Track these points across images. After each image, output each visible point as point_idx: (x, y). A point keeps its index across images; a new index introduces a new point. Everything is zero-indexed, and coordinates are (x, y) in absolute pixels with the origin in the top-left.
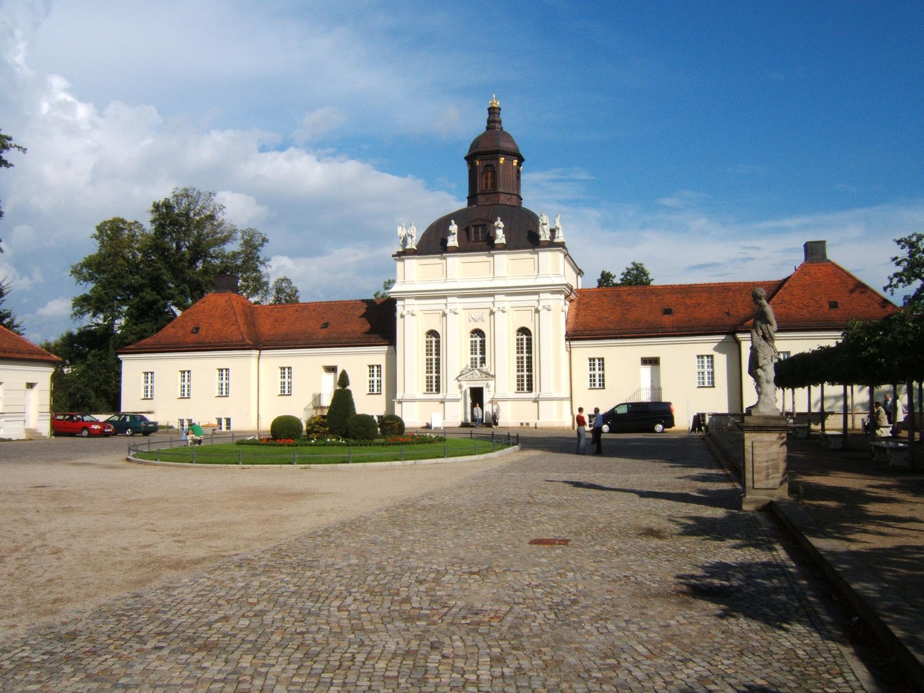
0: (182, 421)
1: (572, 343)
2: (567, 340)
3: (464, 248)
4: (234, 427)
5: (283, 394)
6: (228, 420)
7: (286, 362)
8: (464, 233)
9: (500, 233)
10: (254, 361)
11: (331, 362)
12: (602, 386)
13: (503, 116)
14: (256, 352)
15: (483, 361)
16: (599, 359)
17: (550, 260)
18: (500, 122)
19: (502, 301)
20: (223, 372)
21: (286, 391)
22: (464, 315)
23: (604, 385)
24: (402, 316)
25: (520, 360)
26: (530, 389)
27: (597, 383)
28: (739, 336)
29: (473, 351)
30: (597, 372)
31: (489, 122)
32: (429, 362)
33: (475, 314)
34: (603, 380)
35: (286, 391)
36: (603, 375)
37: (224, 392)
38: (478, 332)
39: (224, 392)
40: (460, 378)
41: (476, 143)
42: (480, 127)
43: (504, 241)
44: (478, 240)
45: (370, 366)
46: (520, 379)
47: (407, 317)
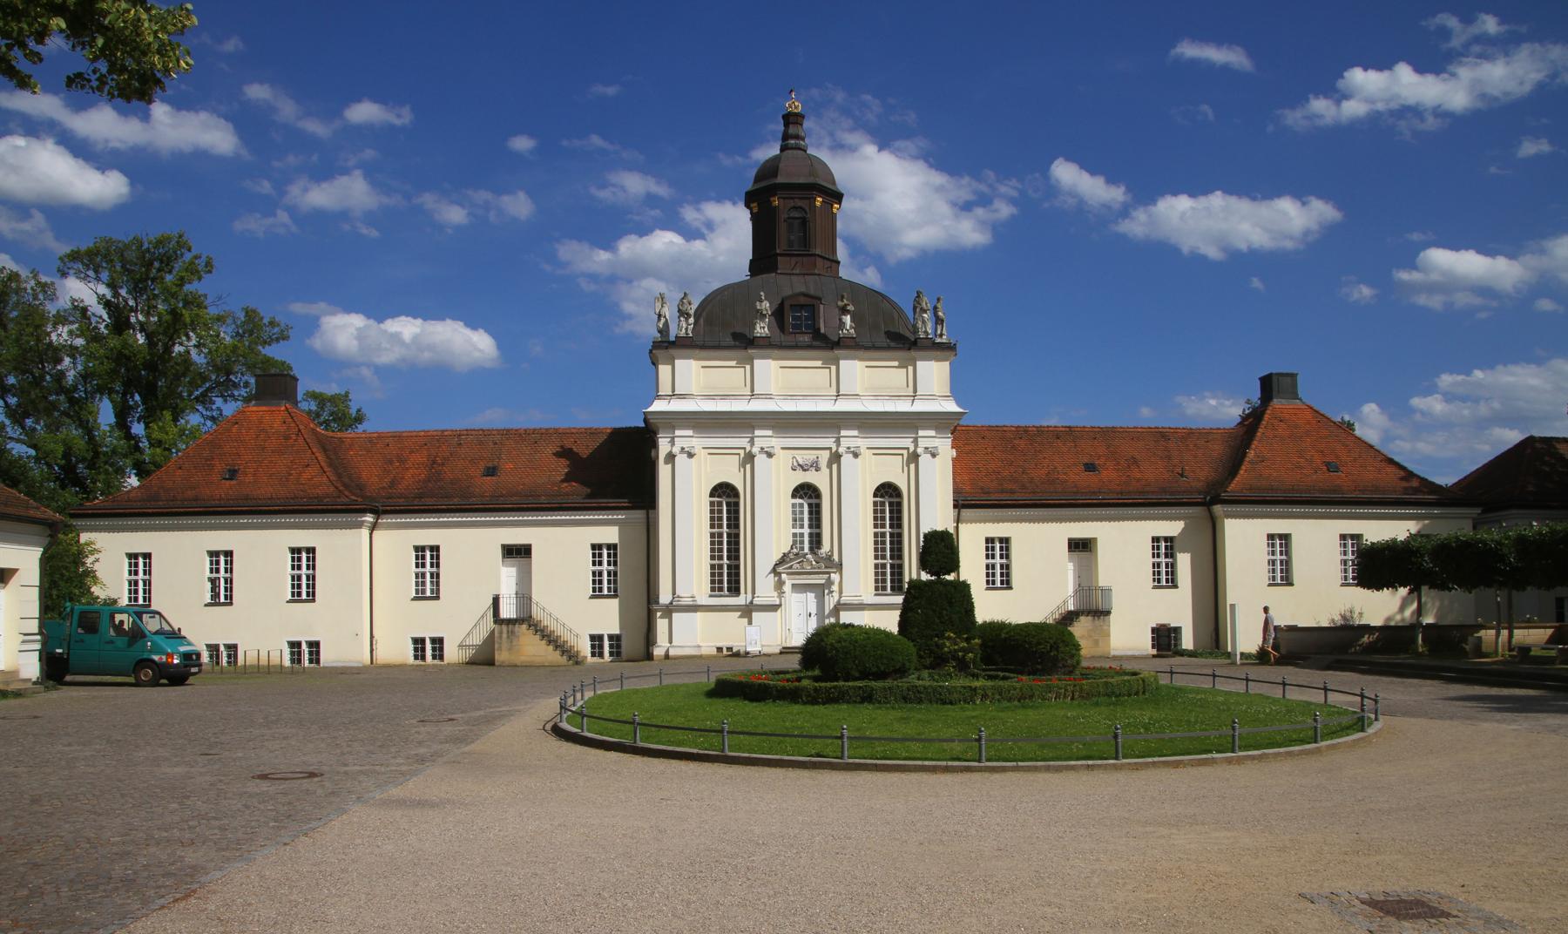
0: (295, 645)
1: (966, 513)
2: (955, 506)
4: (327, 657)
5: (420, 597)
6: (315, 646)
7: (427, 537)
8: (779, 315)
9: (847, 319)
10: (365, 532)
11: (517, 536)
12: (1007, 584)
14: (369, 518)
16: (1001, 540)
17: (934, 374)
19: (851, 438)
20: (303, 556)
21: (428, 586)
22: (783, 459)
23: (1008, 582)
24: (671, 458)
25: (879, 539)
26: (735, 589)
27: (998, 579)
28: (1218, 509)
30: (998, 561)
33: (805, 457)
34: (1008, 575)
35: (428, 586)
36: (1008, 567)
37: (304, 590)
38: (807, 492)
39: (304, 590)
40: (780, 569)
44: (805, 329)
45: (594, 547)
46: (715, 571)
47: (681, 459)
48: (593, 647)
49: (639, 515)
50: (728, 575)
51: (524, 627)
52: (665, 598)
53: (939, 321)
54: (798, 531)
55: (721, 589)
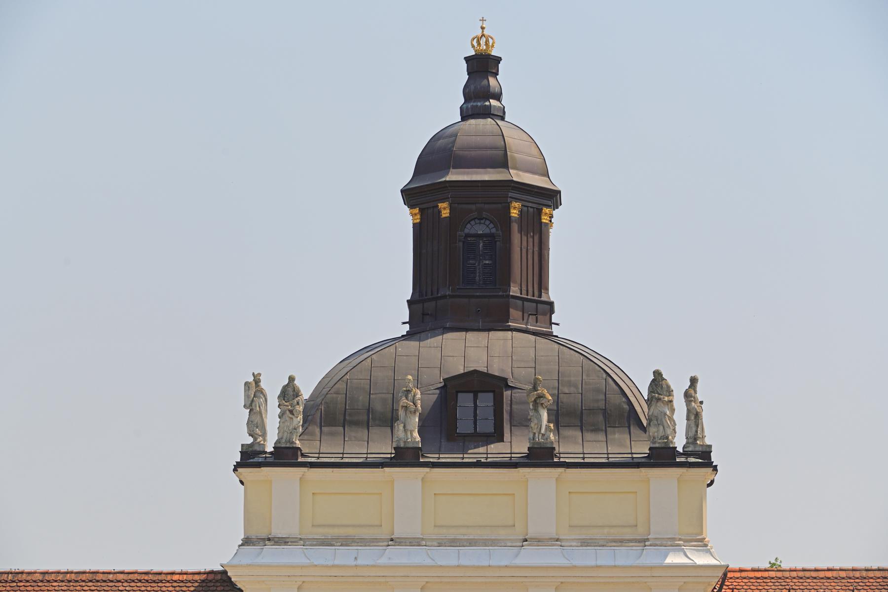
13: (505, 79)
18: (498, 97)
31: (469, 94)
41: (437, 156)
42: (445, 109)
53: (694, 417)
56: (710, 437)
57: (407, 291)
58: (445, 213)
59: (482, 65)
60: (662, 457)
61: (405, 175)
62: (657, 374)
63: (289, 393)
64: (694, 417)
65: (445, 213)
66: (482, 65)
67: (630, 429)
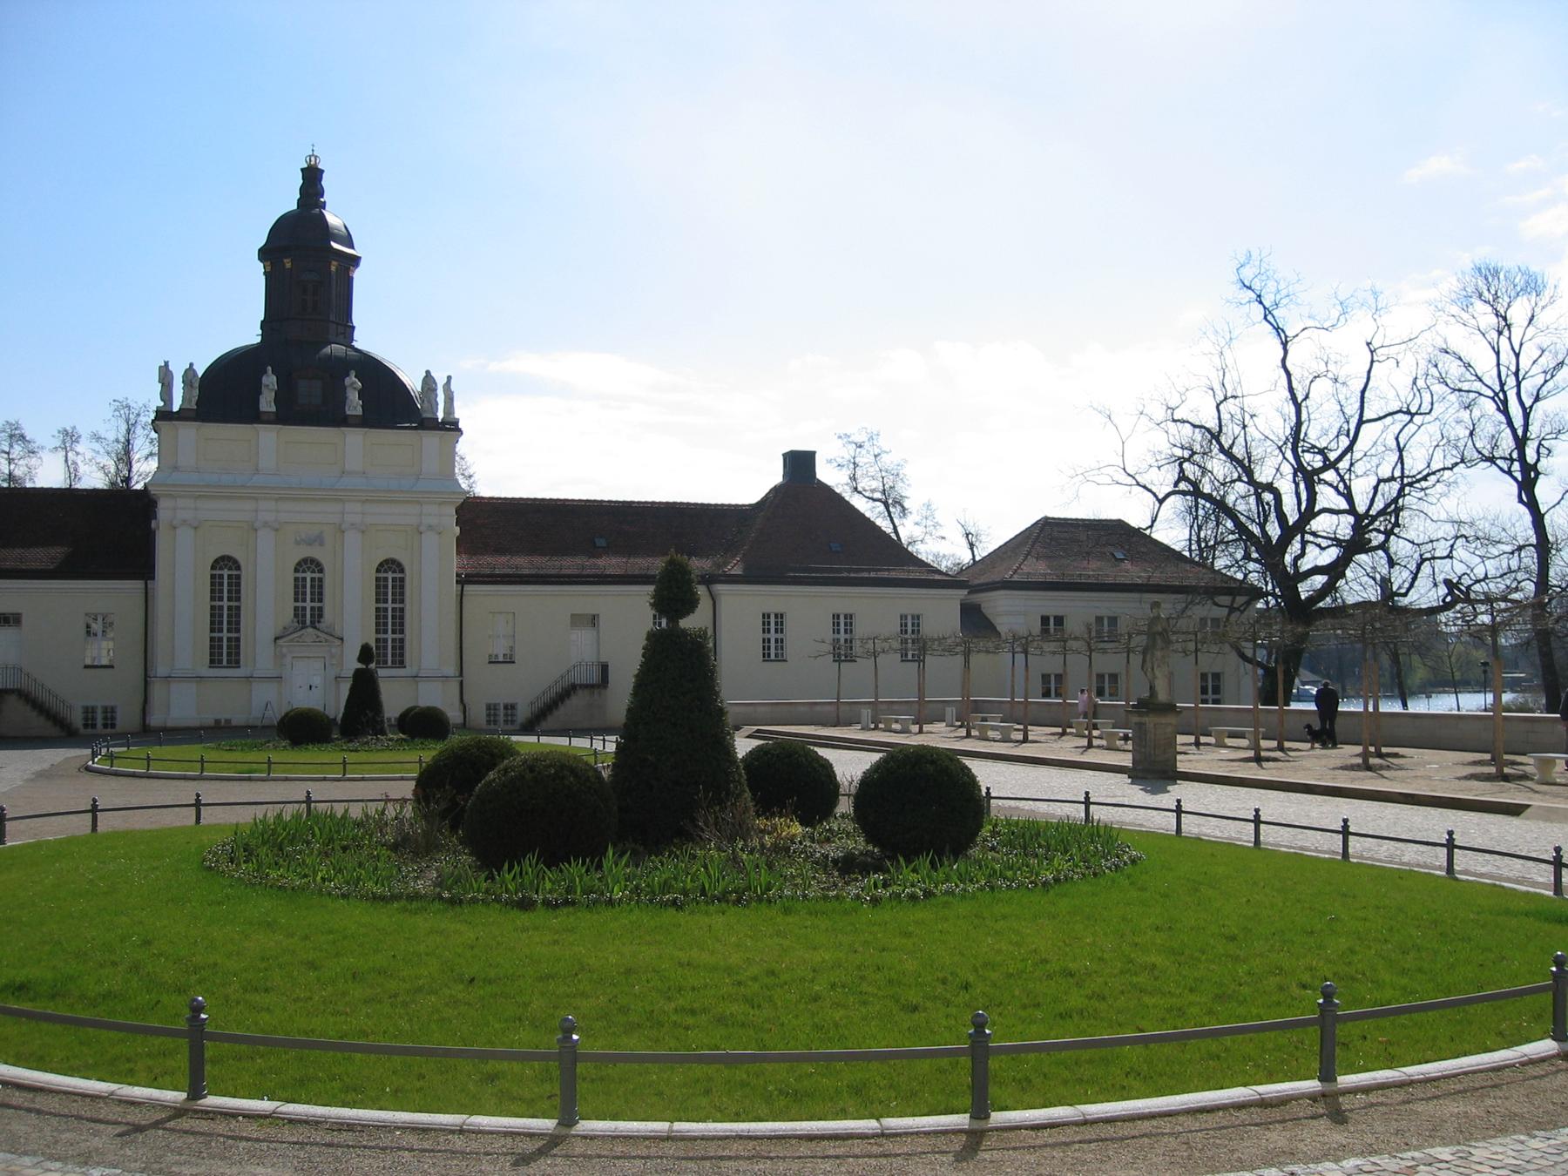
1: (467, 587)
3: (289, 414)
15: (318, 614)
28: (719, 588)
29: (299, 594)
31: (303, 190)
32: (215, 613)
40: (280, 642)
42: (289, 202)
43: (359, 411)
48: (86, 719)
49: (139, 584)
50: (225, 648)
51: (12, 699)
52: (161, 669)
54: (300, 604)
55: (220, 661)
56: (459, 413)
57: (261, 315)
58: (288, 266)
59: (312, 177)
60: (430, 424)
61: (262, 241)
62: (428, 372)
63: (190, 370)
64: (449, 399)
65: (288, 266)
66: (312, 177)
67: (394, 405)
